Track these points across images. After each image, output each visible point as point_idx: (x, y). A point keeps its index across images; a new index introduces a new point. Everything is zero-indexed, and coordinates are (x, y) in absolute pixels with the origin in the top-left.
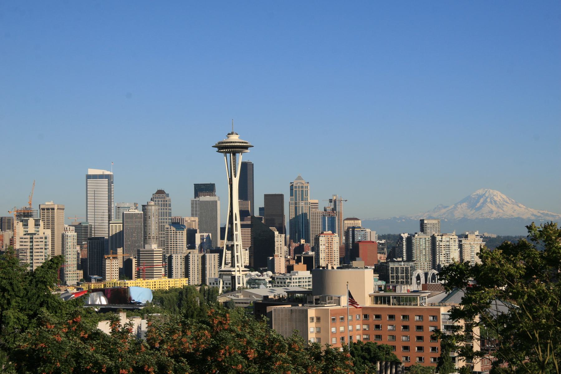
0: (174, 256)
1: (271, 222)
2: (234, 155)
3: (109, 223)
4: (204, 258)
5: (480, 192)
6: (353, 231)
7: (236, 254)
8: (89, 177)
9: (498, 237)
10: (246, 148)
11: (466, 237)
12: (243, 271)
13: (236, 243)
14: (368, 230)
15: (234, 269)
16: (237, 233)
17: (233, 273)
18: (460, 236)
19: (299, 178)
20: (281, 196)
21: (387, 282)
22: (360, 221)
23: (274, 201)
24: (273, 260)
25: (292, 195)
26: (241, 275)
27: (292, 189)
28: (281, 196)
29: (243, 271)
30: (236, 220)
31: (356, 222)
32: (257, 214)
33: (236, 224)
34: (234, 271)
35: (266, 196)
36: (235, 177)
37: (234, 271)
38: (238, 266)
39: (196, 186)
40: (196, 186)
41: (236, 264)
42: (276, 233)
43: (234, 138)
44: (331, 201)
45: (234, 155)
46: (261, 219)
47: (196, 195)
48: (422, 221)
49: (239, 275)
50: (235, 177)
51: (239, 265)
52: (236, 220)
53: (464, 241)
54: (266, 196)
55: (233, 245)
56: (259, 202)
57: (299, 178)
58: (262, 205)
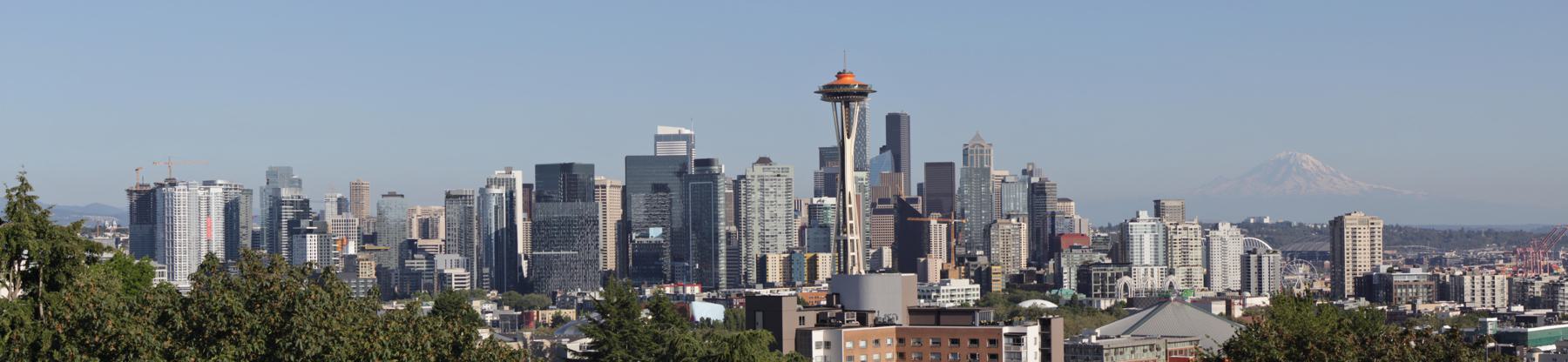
0: (770, 256)
1: (932, 207)
2: (847, 105)
4: (815, 259)
5: (1283, 155)
6: (1053, 219)
7: (850, 254)
8: (659, 138)
9: (1300, 225)
10: (865, 94)
11: (1216, 227)
13: (850, 238)
14: (1077, 217)
18: (1203, 226)
19: (978, 136)
20: (951, 165)
21: (1089, 295)
23: (939, 172)
24: (925, 263)
25: (965, 163)
27: (965, 155)
28: (951, 165)
32: (914, 193)
35: (928, 165)
39: (821, 149)
40: (821, 149)
42: (933, 222)
43: (848, 80)
44: (1024, 172)
45: (847, 105)
46: (915, 201)
47: (822, 164)
48: (1157, 202)
53: (1212, 233)
54: (928, 165)
55: (845, 241)
56: (918, 175)
57: (978, 136)
58: (922, 179)
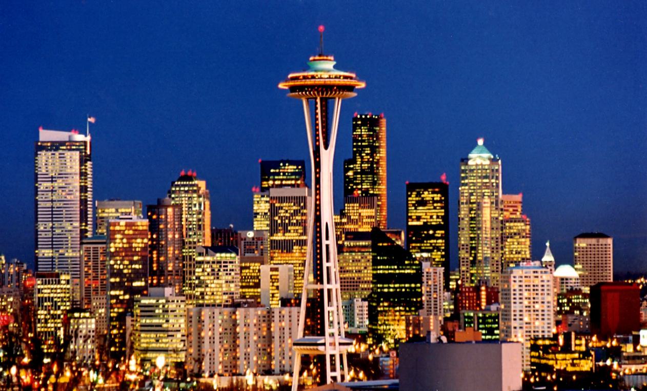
3: (82, 244)
12: (340, 344)
13: (326, 286)
15: (322, 341)
16: (328, 264)
17: (321, 348)
22: (610, 241)
26: (337, 353)
29: (340, 344)
30: (327, 238)
31: (602, 241)
33: (327, 246)
34: (324, 344)
36: (326, 147)
37: (324, 344)
38: (332, 335)
41: (328, 330)
49: (333, 352)
50: (326, 147)
51: (335, 330)
52: (327, 238)
55: (322, 291)
